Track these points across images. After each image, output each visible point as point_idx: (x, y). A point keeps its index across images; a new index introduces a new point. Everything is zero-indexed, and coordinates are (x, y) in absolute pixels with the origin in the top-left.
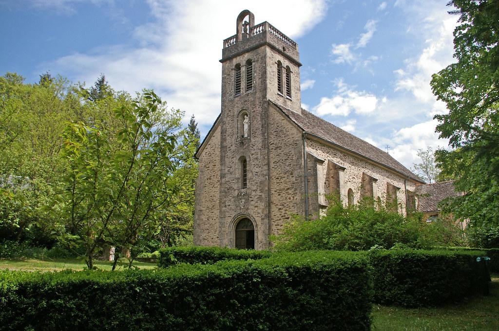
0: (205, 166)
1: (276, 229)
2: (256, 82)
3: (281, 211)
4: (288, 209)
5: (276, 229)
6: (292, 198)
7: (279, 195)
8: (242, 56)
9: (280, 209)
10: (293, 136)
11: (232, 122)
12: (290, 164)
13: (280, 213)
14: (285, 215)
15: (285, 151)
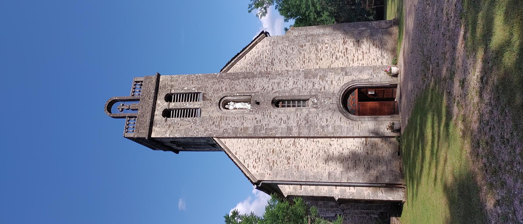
0: (271, 169)
1: (357, 62)
2: (194, 87)
3: (338, 57)
5: (357, 62)
6: (327, 45)
7: (321, 59)
8: (157, 107)
9: (336, 58)
10: (265, 46)
11: (228, 120)
12: (292, 48)
13: (341, 58)
14: (343, 52)
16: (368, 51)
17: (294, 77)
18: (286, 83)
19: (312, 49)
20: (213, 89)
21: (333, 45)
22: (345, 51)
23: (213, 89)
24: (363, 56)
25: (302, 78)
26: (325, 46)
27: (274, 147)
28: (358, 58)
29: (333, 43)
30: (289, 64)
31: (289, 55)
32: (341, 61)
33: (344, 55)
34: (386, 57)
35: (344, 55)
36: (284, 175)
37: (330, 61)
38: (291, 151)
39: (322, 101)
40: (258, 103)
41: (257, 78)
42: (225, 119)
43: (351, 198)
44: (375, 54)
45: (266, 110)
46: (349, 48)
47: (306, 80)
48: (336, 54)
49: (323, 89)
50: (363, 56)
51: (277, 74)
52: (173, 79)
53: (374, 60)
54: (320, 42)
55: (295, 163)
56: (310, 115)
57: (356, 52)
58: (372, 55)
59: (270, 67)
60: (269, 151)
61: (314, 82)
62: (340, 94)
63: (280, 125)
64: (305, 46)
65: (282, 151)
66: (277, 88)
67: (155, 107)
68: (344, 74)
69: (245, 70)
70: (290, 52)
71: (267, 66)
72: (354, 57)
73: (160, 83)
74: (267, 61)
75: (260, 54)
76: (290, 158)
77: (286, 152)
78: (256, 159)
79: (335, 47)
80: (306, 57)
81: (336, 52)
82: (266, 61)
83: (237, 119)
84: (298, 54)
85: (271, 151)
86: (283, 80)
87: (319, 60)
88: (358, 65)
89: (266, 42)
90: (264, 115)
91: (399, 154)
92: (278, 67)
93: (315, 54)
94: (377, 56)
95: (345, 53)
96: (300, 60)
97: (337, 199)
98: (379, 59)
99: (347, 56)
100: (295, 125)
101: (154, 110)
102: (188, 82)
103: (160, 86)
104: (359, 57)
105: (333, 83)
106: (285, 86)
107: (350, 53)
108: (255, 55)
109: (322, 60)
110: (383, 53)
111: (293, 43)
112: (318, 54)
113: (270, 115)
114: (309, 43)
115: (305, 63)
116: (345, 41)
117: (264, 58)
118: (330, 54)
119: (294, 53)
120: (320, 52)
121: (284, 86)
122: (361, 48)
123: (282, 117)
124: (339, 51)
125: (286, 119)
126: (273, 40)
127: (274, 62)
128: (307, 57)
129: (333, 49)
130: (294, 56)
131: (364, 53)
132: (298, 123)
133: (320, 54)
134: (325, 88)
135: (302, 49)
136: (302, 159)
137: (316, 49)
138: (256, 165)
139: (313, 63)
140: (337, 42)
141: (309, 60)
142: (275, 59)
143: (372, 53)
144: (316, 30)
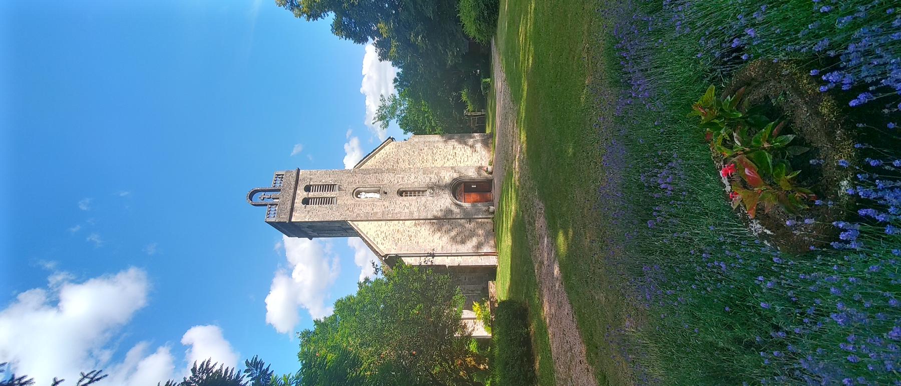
0: (396, 245)
2: (331, 180)
4: (448, 153)
6: (440, 150)
7: (436, 160)
9: (448, 160)
15: (402, 156)
16: (471, 155)
21: (445, 150)
27: (399, 228)
36: (406, 249)
40: (386, 193)
49: (437, 182)
56: (428, 202)
60: (394, 231)
73: (300, 176)
77: (408, 231)
85: (397, 231)
92: (402, 165)
97: (447, 266)
100: (416, 210)
102: (326, 176)
119: (415, 155)
138: (383, 242)
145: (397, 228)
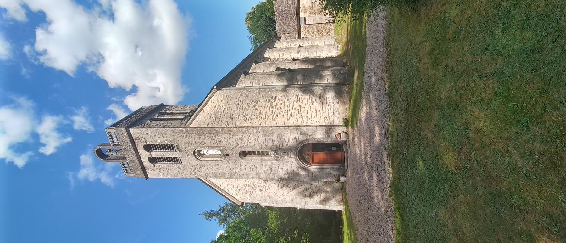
0: (250, 196)
1: (311, 119)
3: (293, 114)
4: (291, 107)
5: (311, 119)
6: (281, 102)
8: (141, 155)
9: (291, 115)
10: (220, 100)
11: (206, 167)
12: (248, 103)
13: (295, 115)
14: (297, 109)
15: (235, 110)
16: (321, 109)
17: (254, 134)
18: (248, 139)
19: (267, 105)
20: (183, 142)
21: (287, 102)
22: (299, 108)
23: (183, 142)
24: (316, 114)
25: (262, 135)
26: (279, 103)
27: (249, 183)
28: (311, 116)
29: (287, 100)
30: (247, 120)
31: (246, 110)
32: (296, 118)
33: (299, 112)
34: (338, 116)
35: (299, 112)
36: (260, 199)
37: (286, 117)
38: (262, 186)
39: (282, 155)
40: (227, 155)
41: (221, 135)
42: (204, 166)
43: (308, 208)
44: (327, 112)
45: (236, 161)
46: (303, 106)
47: (265, 137)
48: (290, 112)
49: (281, 145)
50: (316, 114)
51: (238, 132)
52: (143, 132)
53: (327, 118)
54: (274, 98)
55: (266, 193)
56: (273, 166)
57: (310, 110)
58: (325, 113)
59: (230, 122)
60: (245, 185)
61: (273, 140)
62: (296, 150)
63: (250, 172)
64: (260, 102)
65: (256, 186)
66: (241, 144)
67: (140, 156)
68: (299, 134)
69: (207, 123)
70: (246, 108)
71: (227, 120)
72: (308, 114)
73: (133, 135)
74: (226, 116)
75: (217, 108)
76: (262, 190)
77: (259, 186)
78: (237, 190)
79: (289, 104)
80: (262, 113)
81: (290, 109)
82: (225, 116)
83: (213, 166)
84: (254, 110)
85: (247, 185)
86: (245, 137)
87: (275, 117)
88: (312, 122)
89: (220, 96)
90: (235, 164)
91: (342, 188)
92: (238, 122)
93: (270, 111)
94: (329, 115)
95: (299, 111)
96: (257, 116)
97: (299, 209)
98: (331, 117)
99: (301, 113)
100: (262, 172)
101: (140, 158)
102: (159, 136)
103: (134, 138)
104: (312, 114)
105: (290, 141)
106: (247, 142)
107: (304, 110)
108: (212, 109)
109: (278, 117)
110: (335, 112)
111: (247, 99)
112: (273, 111)
113: (240, 165)
114: (263, 99)
115: (263, 119)
116: (299, 99)
117: (223, 113)
118: (285, 111)
119: (250, 108)
120: (275, 108)
121: (246, 142)
122: (314, 105)
123: (251, 166)
124: (293, 108)
125: (254, 168)
126: (226, 95)
127: (233, 117)
128: (263, 113)
129: (287, 106)
130: (250, 112)
131: (317, 111)
132: (264, 171)
133: (275, 110)
134: (284, 145)
135: (257, 104)
136: (271, 190)
137: (271, 105)
138: (238, 193)
139: (270, 119)
140: (290, 99)
141: (266, 116)
142: (233, 114)
143: (324, 111)
144: (268, 80)
145: (247, 183)
